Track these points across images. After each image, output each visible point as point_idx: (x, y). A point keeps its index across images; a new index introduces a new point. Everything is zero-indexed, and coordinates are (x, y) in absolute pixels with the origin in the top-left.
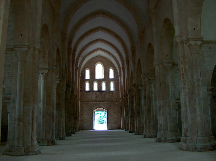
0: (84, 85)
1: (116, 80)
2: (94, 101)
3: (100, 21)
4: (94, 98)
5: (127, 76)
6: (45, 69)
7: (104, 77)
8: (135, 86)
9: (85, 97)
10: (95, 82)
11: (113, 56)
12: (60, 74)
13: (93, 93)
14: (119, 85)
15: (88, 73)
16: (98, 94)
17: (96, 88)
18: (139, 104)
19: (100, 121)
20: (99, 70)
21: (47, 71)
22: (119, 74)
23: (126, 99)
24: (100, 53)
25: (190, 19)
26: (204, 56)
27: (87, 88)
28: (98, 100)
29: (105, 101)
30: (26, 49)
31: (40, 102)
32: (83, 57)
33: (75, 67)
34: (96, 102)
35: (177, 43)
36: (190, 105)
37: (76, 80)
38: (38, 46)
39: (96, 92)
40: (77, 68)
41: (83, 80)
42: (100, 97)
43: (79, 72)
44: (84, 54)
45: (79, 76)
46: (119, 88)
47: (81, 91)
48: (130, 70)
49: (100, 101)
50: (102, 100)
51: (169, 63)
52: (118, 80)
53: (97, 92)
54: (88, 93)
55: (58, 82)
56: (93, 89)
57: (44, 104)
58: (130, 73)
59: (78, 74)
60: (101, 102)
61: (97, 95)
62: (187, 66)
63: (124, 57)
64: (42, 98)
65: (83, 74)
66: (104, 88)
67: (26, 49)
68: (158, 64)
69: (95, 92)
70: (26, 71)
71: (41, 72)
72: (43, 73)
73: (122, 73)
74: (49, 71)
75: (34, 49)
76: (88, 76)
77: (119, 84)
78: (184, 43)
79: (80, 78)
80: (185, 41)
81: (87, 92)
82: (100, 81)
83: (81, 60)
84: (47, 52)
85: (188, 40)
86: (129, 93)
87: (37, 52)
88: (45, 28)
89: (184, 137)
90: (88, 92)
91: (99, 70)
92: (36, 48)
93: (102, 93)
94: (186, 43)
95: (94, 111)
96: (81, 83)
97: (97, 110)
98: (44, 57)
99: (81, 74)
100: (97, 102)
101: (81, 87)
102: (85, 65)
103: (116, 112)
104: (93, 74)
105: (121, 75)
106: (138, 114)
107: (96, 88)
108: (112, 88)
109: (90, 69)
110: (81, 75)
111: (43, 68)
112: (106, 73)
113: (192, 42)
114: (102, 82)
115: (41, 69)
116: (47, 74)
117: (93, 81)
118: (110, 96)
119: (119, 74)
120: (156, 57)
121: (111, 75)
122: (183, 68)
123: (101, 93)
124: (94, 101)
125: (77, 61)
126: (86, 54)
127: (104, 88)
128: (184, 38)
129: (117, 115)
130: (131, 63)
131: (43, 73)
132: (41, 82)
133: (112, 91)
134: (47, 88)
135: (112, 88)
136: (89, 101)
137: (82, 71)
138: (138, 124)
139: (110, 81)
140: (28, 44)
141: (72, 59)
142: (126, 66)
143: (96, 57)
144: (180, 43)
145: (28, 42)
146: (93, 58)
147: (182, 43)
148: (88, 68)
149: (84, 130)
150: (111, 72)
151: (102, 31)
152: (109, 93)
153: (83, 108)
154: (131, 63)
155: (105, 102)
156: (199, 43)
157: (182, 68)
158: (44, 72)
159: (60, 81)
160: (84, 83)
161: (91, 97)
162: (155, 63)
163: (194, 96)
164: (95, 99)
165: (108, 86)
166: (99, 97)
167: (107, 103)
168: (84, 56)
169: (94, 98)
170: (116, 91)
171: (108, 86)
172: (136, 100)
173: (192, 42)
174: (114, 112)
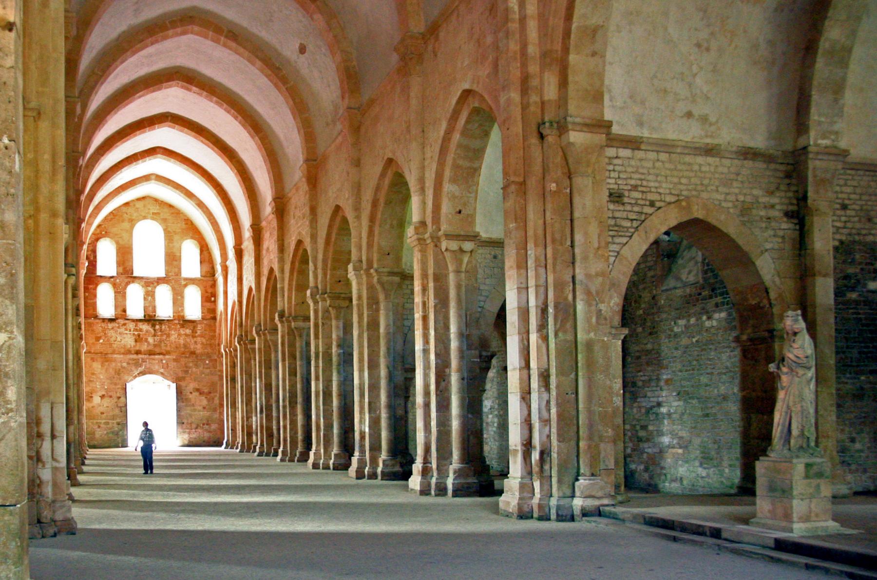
0: (95, 296)
2: (129, 352)
7: (167, 272)
8: (281, 316)
9: (98, 339)
11: (201, 205)
13: (125, 324)
14: (215, 302)
16: (145, 327)
17: (135, 309)
26: (479, 276)
28: (144, 347)
29: (168, 353)
34: (135, 356)
42: (151, 340)
46: (213, 311)
48: (265, 263)
49: (151, 353)
51: (392, 274)
52: (214, 285)
53: (140, 320)
54: (110, 325)
56: (124, 311)
58: (265, 272)
60: (152, 357)
61: (141, 330)
63: (246, 219)
69: (133, 320)
81: (104, 320)
82: (150, 284)
86: (259, 335)
90: (111, 320)
93: (157, 327)
100: (140, 356)
102: (99, 226)
107: (135, 309)
108: (193, 309)
109: (117, 243)
110: (87, 264)
112: (173, 259)
117: (128, 284)
118: (186, 335)
121: (191, 264)
123: (154, 326)
124: (129, 352)
127: (164, 310)
130: (270, 243)
136: (114, 353)
138: (291, 429)
139: (186, 286)
142: (248, 245)
146: (127, 204)
150: (190, 252)
151: (174, 128)
152: (182, 326)
153: (93, 374)
154: (270, 243)
155: (167, 357)
156: (468, 246)
160: (95, 289)
161: (119, 339)
163: (447, 370)
164: (133, 343)
165: (178, 300)
166: (146, 340)
169: (129, 341)
171: (178, 300)
172: (284, 360)
174: (198, 390)
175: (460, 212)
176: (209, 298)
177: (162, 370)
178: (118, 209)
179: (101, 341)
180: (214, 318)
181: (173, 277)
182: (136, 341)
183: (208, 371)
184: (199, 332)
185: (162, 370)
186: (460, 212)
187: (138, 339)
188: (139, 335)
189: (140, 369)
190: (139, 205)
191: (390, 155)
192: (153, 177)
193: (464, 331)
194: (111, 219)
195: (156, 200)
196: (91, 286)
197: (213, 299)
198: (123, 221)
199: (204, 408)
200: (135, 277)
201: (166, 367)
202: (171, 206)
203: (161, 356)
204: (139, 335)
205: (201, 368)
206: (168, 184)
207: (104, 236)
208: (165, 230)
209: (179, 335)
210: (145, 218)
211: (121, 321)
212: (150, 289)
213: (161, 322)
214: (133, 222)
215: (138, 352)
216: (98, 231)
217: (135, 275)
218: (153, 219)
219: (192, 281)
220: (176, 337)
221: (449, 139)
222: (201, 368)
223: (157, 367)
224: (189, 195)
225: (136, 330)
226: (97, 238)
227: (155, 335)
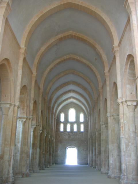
1: (86, 123)
3: (71, 77)
6: (24, 118)
7: (76, 120)
10: (68, 124)
12: (36, 120)
14: (87, 127)
15: (62, 116)
16: (71, 134)
17: (69, 129)
18: (100, 145)
19: (72, 157)
20: (72, 113)
21: (25, 120)
22: (87, 118)
23: (92, 139)
25: (128, 86)
27: (62, 129)
30: (8, 106)
31: (19, 143)
35: (119, 103)
36: (127, 151)
37: (52, 123)
38: (17, 103)
39: (69, 132)
40: (52, 113)
41: (58, 122)
42: (72, 137)
43: (55, 116)
44: (59, 102)
47: (57, 131)
50: (74, 139)
54: (63, 133)
55: (35, 126)
57: (21, 145)
59: (54, 117)
61: (70, 135)
62: (125, 122)
64: (20, 140)
65: (59, 118)
66: (75, 129)
67: (8, 106)
68: (110, 116)
70: (8, 122)
71: (21, 120)
72: (22, 121)
73: (89, 117)
74: (27, 119)
75: (15, 106)
76: (62, 119)
77: (87, 126)
78: (124, 104)
80: (124, 102)
82: (72, 124)
84: (26, 105)
85: (126, 101)
87: (16, 108)
88: (24, 88)
91: (72, 113)
92: (16, 105)
94: (125, 104)
95: (66, 149)
96: (57, 125)
97: (69, 148)
98: (23, 109)
101: (57, 128)
103: (85, 150)
106: (99, 154)
107: (69, 129)
108: (82, 129)
110: (56, 118)
111: (22, 117)
112: (78, 117)
113: (129, 103)
115: (20, 118)
116: (25, 122)
117: (67, 123)
120: (108, 110)
122: (123, 122)
125: (53, 108)
127: (75, 129)
128: (124, 100)
131: (22, 121)
132: (20, 128)
133: (82, 132)
134: (25, 132)
140: (10, 103)
144: (121, 103)
145: (10, 101)
146: (67, 104)
147: (122, 102)
149: (58, 164)
157: (122, 122)
158: (23, 120)
159: (36, 125)
160: (59, 124)
161: (64, 137)
162: (108, 114)
164: (68, 138)
165: (79, 127)
169: (67, 137)
171: (79, 127)
173: (129, 103)
174: (83, 150)
175: (131, 93)
176: (86, 127)
179: (60, 137)
180: (87, 131)
181: (78, 122)
182: (68, 137)
184: (83, 135)
186: (131, 93)
187: (69, 137)
189: (70, 144)
191: (114, 81)
193: (135, 131)
196: (59, 124)
200: (69, 122)
207: (62, 112)
209: (79, 136)
210: (71, 108)
211: (65, 132)
213: (75, 132)
214: (68, 109)
215: (69, 140)
218: (73, 108)
219: (82, 123)
221: (126, 71)
226: (60, 112)
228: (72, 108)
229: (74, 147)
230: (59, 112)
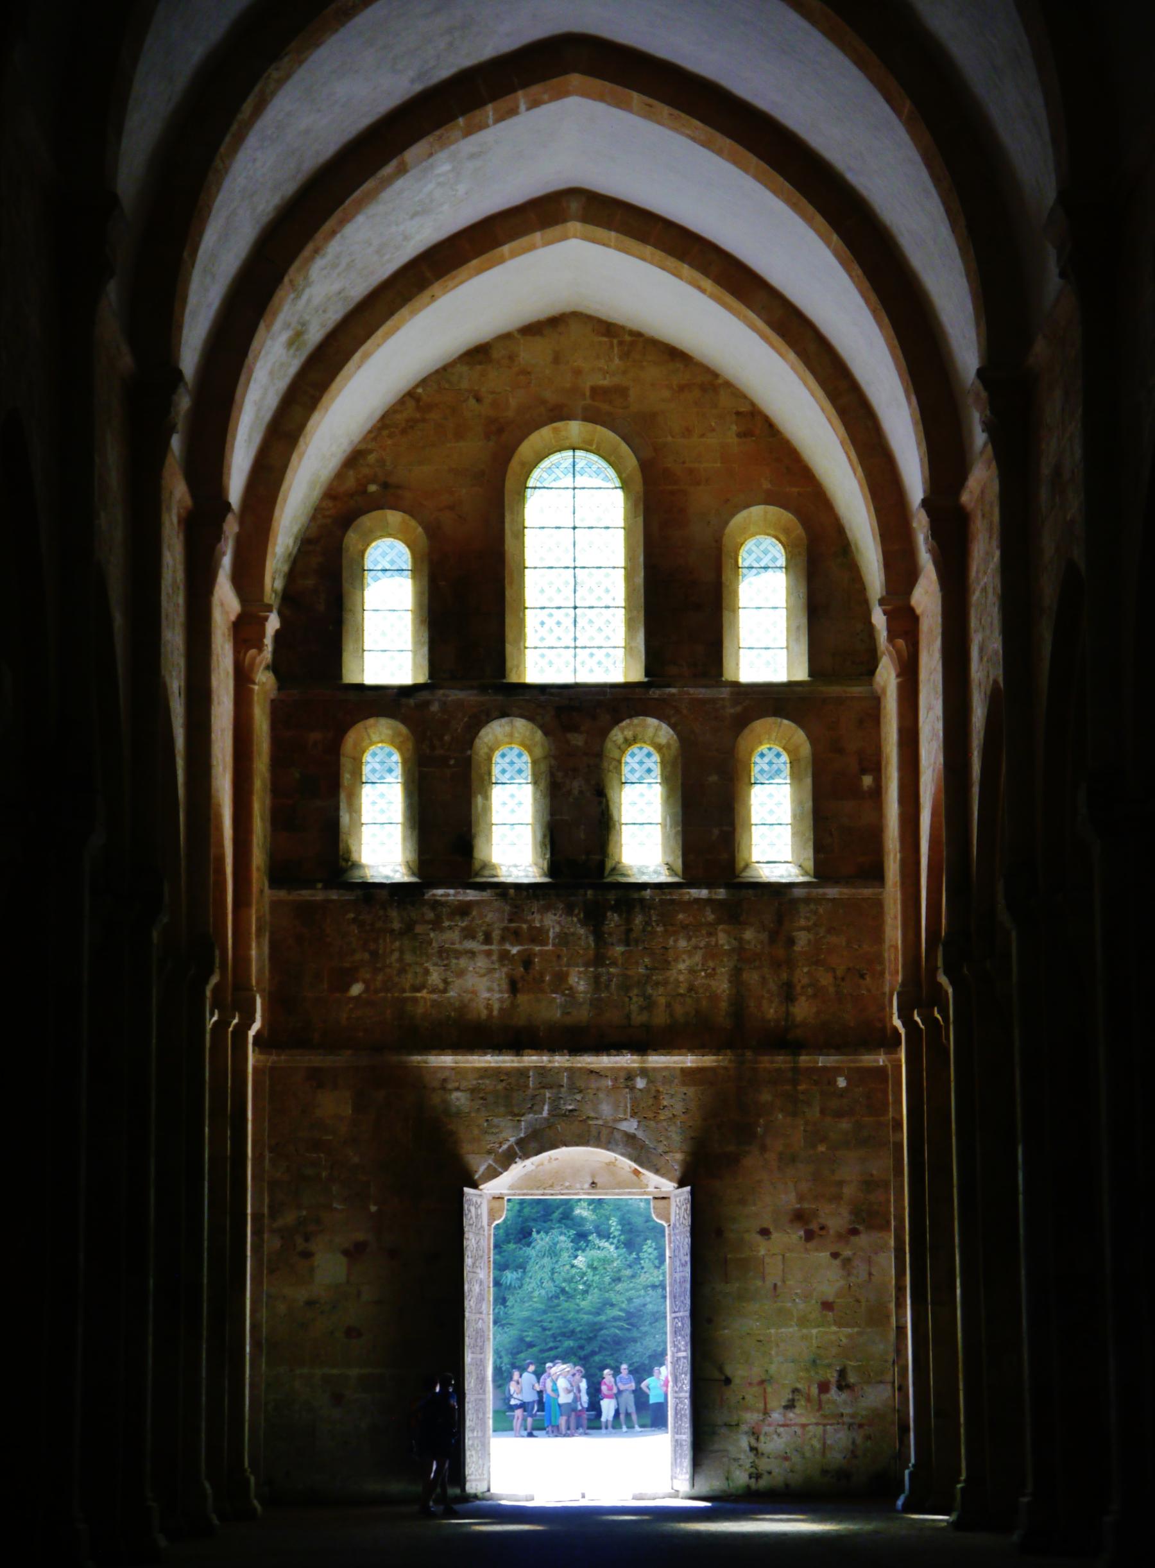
4: (480, 985)
5: (996, 644)
10: (495, 730)
13: (464, 910)
14: (877, 793)
17: (512, 840)
22: (879, 619)
24: (577, 272)
32: (315, 335)
33: (178, 492)
45: (246, 631)
48: (1048, 544)
59: (226, 601)
61: (538, 936)
69: (503, 889)
73: (926, 596)
79: (264, 680)
82: (578, 725)
83: (282, 385)
89: (817, 1424)
93: (613, 920)
99: (290, 599)
101: (283, 819)
102: (354, 459)
103: (835, 1219)
104: (471, 600)
105: (905, 622)
107: (512, 840)
110: (273, 623)
114: (617, 735)
119: (879, 619)
123: (594, 918)
126: (359, 289)
127: (643, 840)
129: (847, 1263)
135: (774, 838)
137: (307, 543)
139: (742, 722)
141: (126, 361)
142: (981, 482)
143: (532, 330)
146: (478, 355)
148: (394, 517)
154: (1061, 444)
155: (656, 1060)
160: (334, 748)
161: (435, 978)
166: (561, 978)
167: (688, 1074)
168: (334, 315)
170: (832, 892)
174: (799, 1217)
177: (630, 1126)
178: (440, 377)
179: (356, 989)
180: (877, 875)
182: (514, 987)
183: (845, 1125)
184: (802, 939)
185: (630, 1126)
188: (527, 962)
190: (533, 354)
192: (574, 206)
194: (411, 424)
195: (608, 329)
197: (867, 781)
198: (459, 435)
199: (827, 1306)
201: (647, 1107)
202: (674, 355)
203: (627, 1060)
204: (527, 962)
205: (814, 1113)
206: (643, 238)
208: (645, 466)
209: (712, 953)
210: (558, 414)
212: (577, 740)
213: (633, 895)
216: (350, 483)
217: (513, 678)
219: (770, 700)
220: (693, 967)
222: (814, 1113)
223: (606, 1109)
224: (736, 281)
225: (516, 936)
227: (599, 960)
228: (575, 428)
229: (626, 1164)
230: (317, 512)
